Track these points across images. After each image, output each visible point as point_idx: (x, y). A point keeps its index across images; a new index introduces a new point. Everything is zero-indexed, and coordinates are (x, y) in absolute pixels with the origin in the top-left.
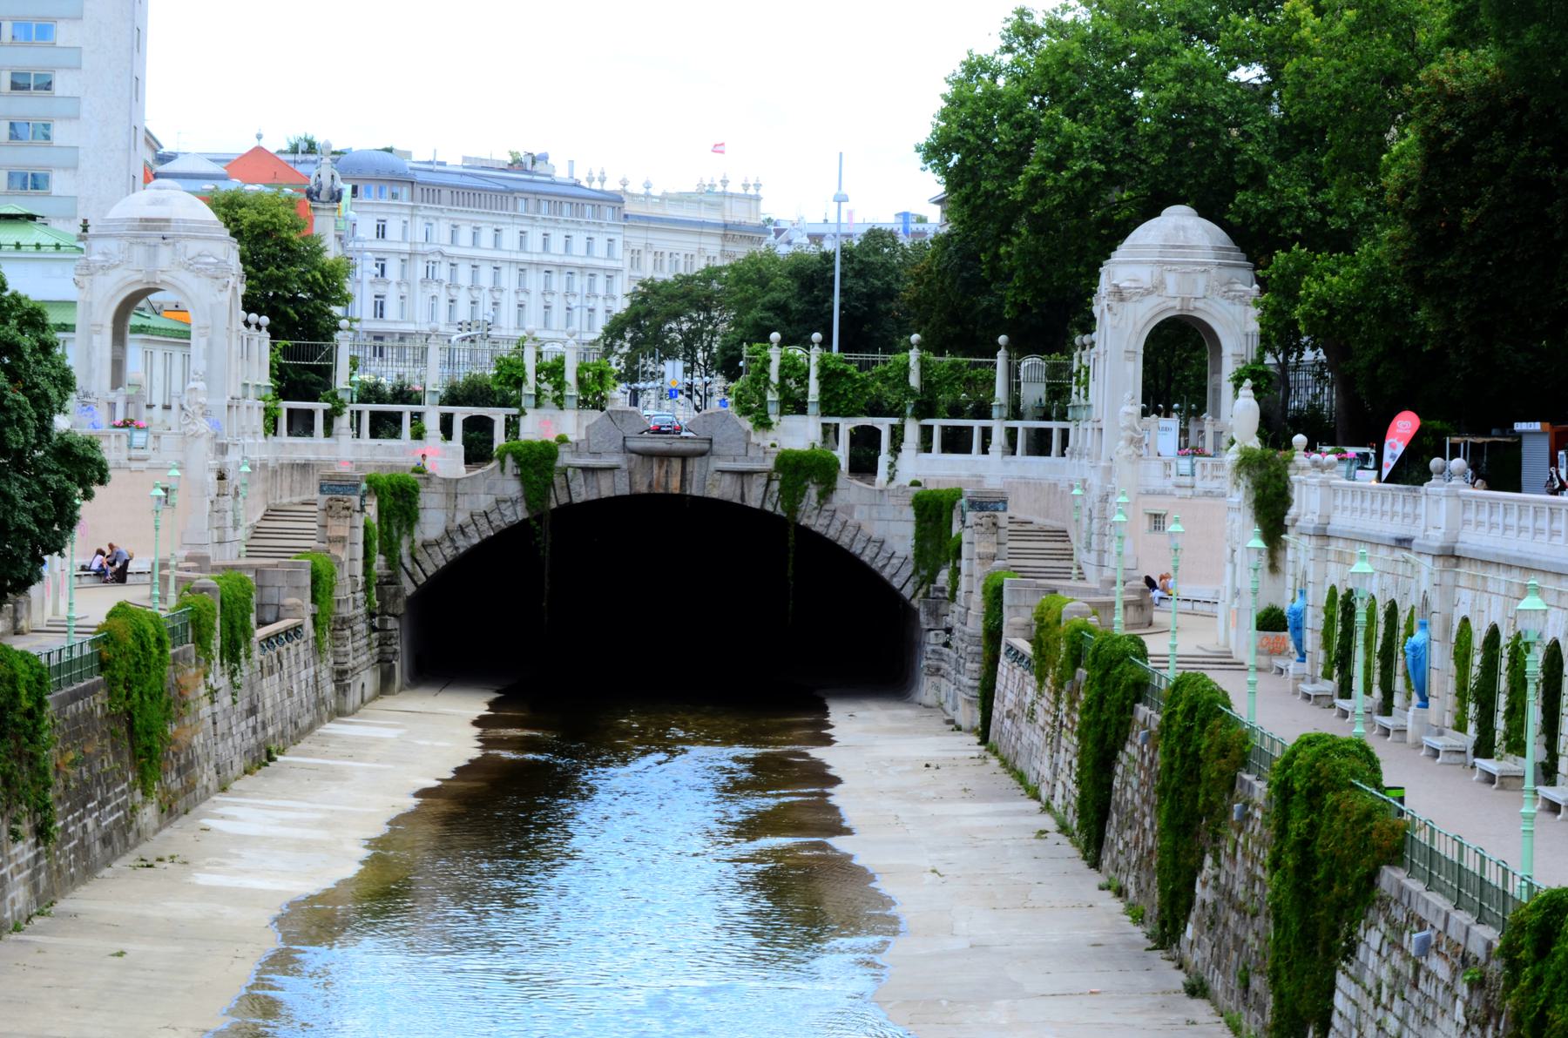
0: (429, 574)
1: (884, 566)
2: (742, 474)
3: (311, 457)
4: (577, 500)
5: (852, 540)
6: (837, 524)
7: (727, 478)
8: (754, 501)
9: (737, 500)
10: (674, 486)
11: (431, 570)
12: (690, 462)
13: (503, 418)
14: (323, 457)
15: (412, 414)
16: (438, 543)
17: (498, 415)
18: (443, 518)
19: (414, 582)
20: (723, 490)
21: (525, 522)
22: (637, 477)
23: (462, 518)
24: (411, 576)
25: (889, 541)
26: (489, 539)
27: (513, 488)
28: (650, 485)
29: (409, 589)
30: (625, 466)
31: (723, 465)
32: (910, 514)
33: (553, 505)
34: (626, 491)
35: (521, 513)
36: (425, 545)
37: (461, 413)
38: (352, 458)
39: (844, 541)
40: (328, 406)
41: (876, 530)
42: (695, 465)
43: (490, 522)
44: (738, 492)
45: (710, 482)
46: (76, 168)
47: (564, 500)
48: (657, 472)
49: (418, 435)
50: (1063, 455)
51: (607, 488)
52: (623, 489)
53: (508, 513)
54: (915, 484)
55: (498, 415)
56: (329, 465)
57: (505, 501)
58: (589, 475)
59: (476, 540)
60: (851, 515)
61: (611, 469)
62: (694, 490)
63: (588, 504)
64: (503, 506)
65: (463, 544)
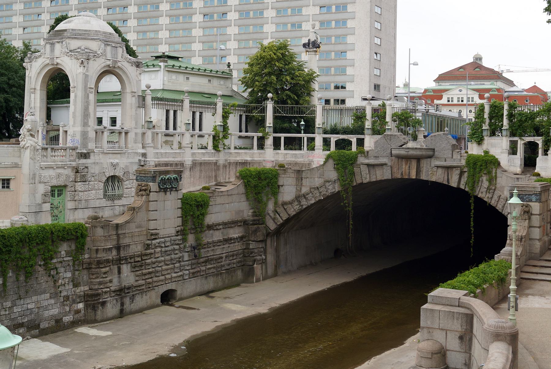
0: (284, 219)
3: (249, 159)
4: (365, 181)
11: (285, 217)
13: (355, 140)
14: (256, 159)
15: (308, 139)
16: (291, 203)
17: (353, 139)
18: (294, 190)
19: (276, 223)
21: (339, 192)
22: (395, 170)
23: (304, 190)
24: (274, 219)
26: (320, 200)
27: (333, 175)
29: (272, 226)
31: (438, 163)
33: (355, 184)
34: (389, 177)
35: (337, 188)
36: (284, 204)
37: (334, 138)
38: (273, 159)
40: (260, 134)
42: (424, 164)
43: (320, 193)
45: (432, 173)
46: (354, 66)
47: (359, 181)
48: (404, 167)
49: (312, 148)
53: (330, 187)
55: (353, 139)
56: (259, 163)
57: (329, 182)
58: (371, 168)
59: (313, 202)
61: (382, 165)
63: (370, 183)
64: (327, 184)
65: (305, 203)
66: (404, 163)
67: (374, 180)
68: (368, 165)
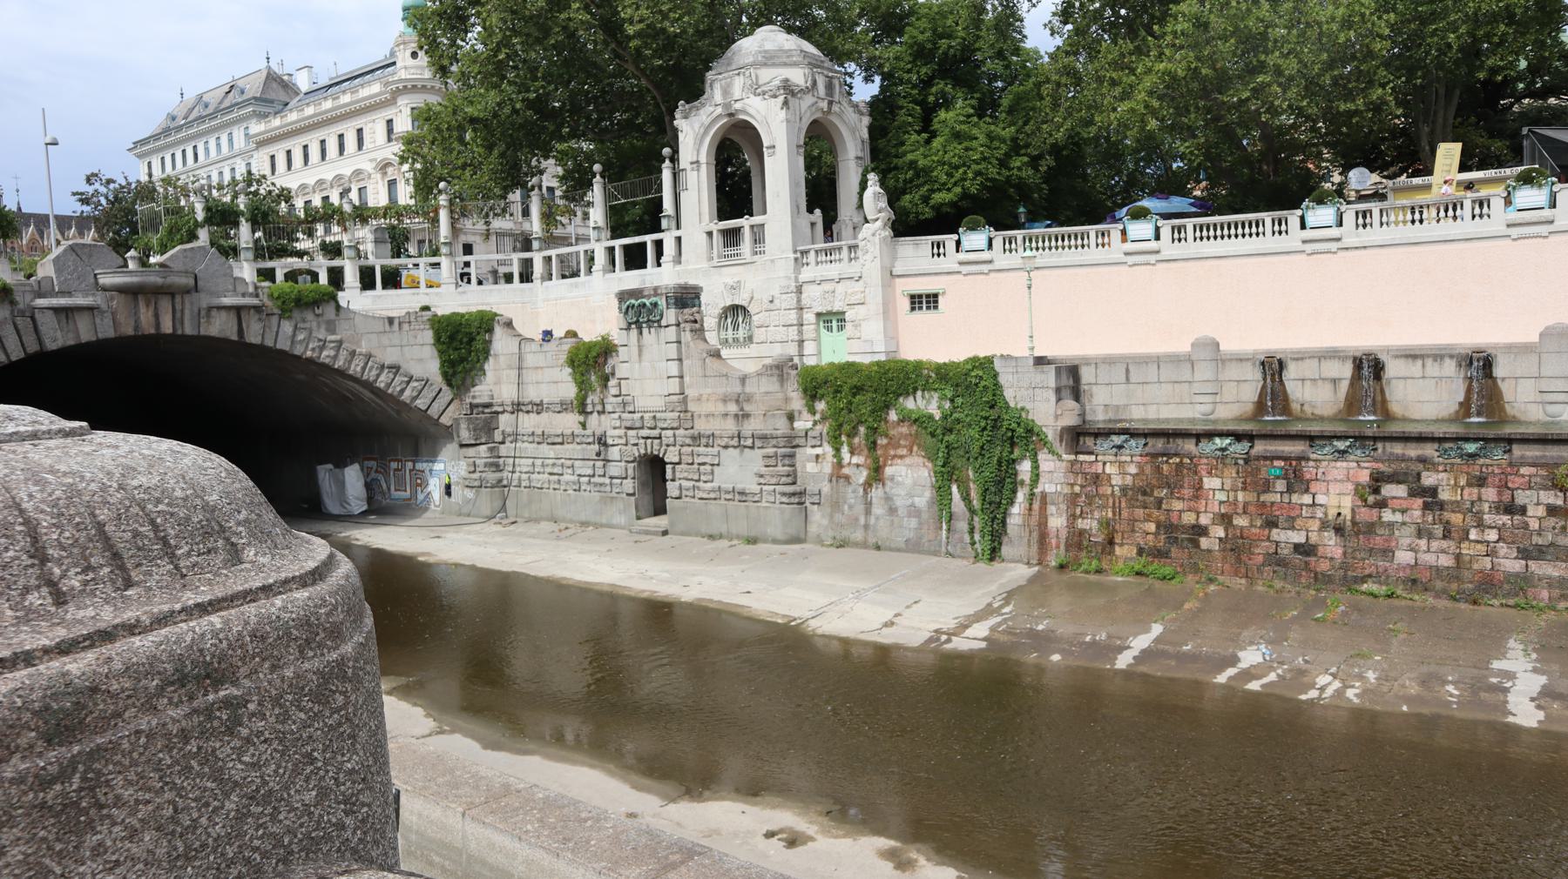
1: (402, 391)
2: (238, 310)
4: (51, 346)
5: (364, 369)
6: (343, 354)
7: (224, 314)
8: (253, 337)
9: (235, 337)
10: (167, 327)
12: (178, 299)
20: (220, 327)
22: (121, 317)
25: (404, 366)
28: (136, 328)
30: (104, 307)
32: (429, 336)
34: (111, 334)
39: (355, 368)
41: (390, 357)
44: (235, 328)
50: (659, 265)
51: (85, 332)
52: (106, 331)
54: (426, 308)
60: (358, 343)
61: (90, 309)
62: (189, 330)
66: (142, 305)
67: (72, 342)
68: (57, 310)
